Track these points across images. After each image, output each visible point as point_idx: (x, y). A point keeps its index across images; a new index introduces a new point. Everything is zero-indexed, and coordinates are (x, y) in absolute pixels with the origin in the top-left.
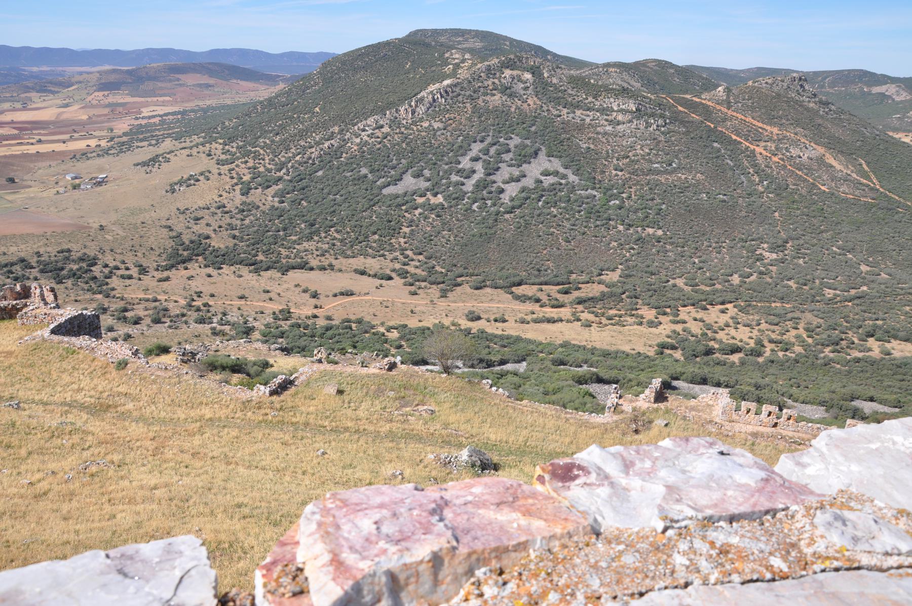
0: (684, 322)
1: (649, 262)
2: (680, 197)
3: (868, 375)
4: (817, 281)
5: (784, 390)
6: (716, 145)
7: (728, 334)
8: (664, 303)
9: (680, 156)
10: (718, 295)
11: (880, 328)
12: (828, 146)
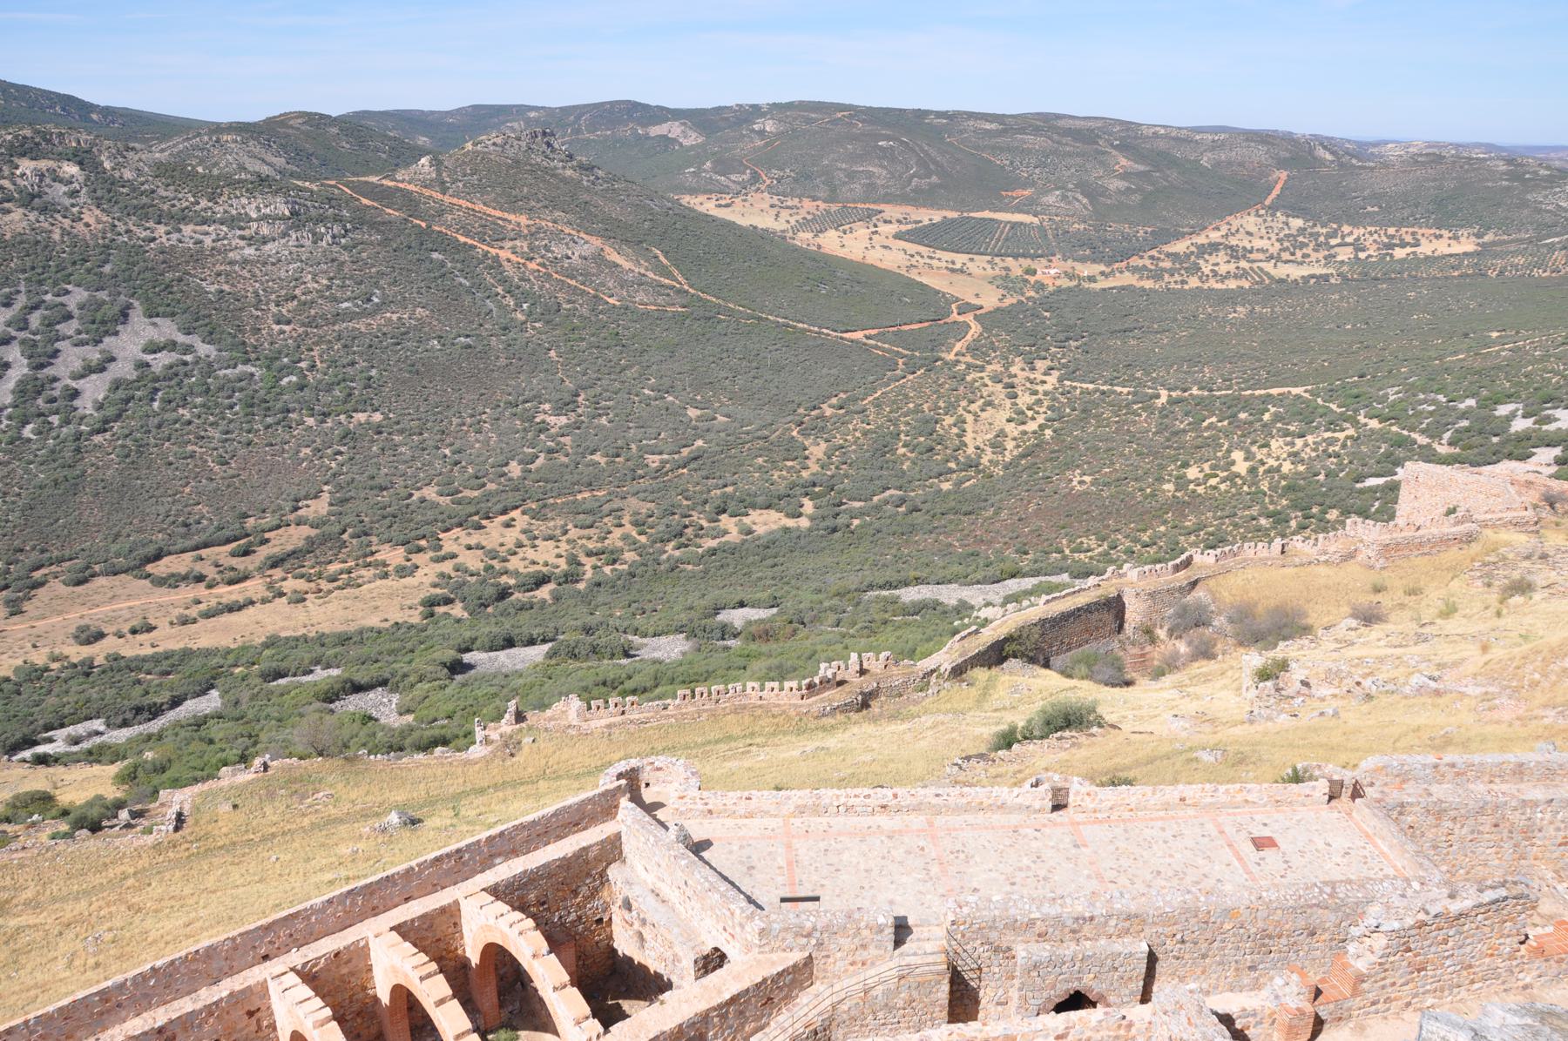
0: (454, 556)
1: (371, 471)
2: (397, 352)
3: (731, 570)
4: (633, 446)
5: (626, 624)
6: (435, 255)
7: (524, 559)
8: (413, 534)
9: (382, 282)
10: (494, 500)
11: (732, 497)
12: (606, 235)
